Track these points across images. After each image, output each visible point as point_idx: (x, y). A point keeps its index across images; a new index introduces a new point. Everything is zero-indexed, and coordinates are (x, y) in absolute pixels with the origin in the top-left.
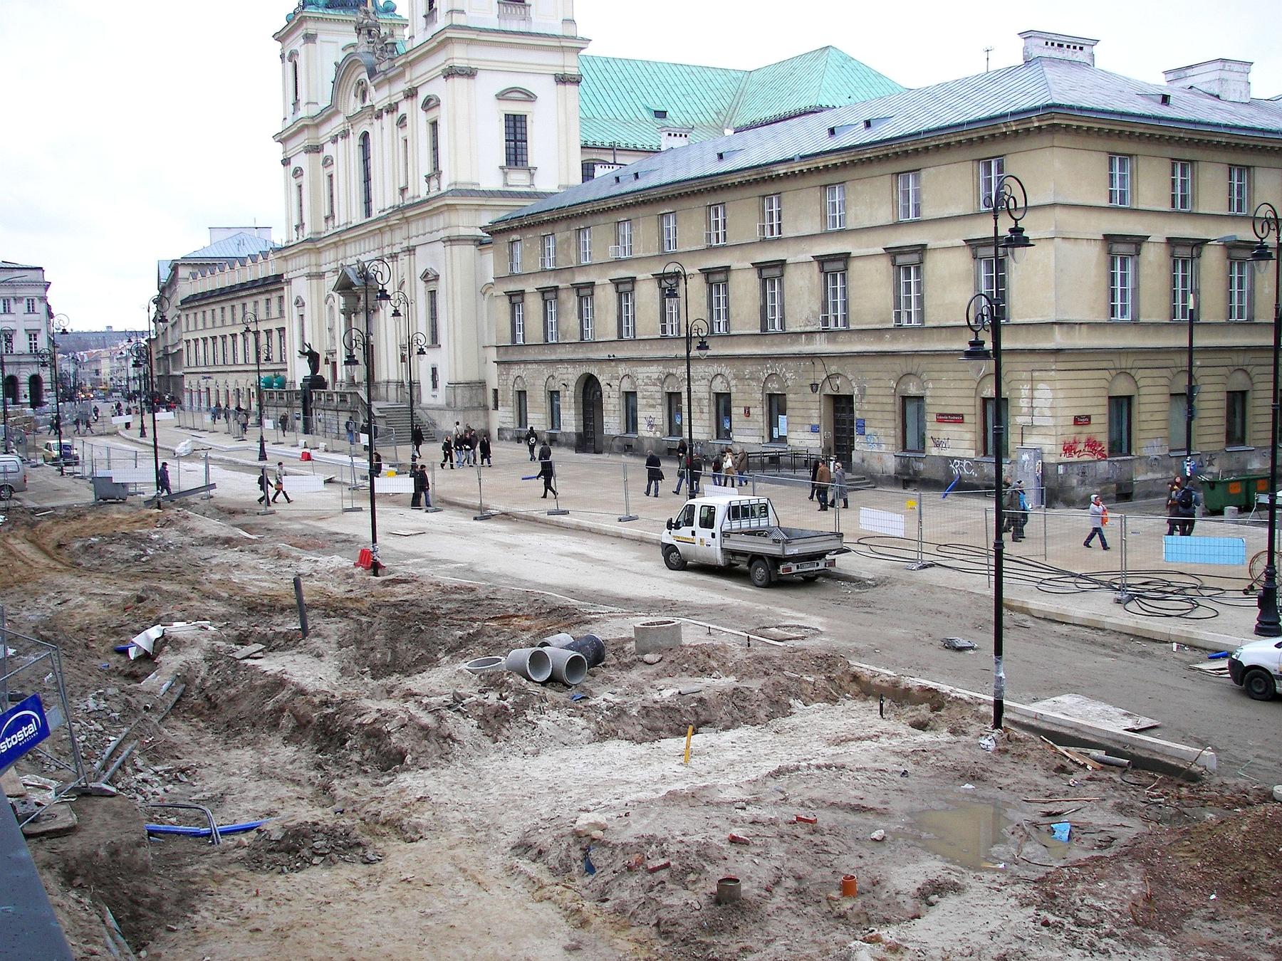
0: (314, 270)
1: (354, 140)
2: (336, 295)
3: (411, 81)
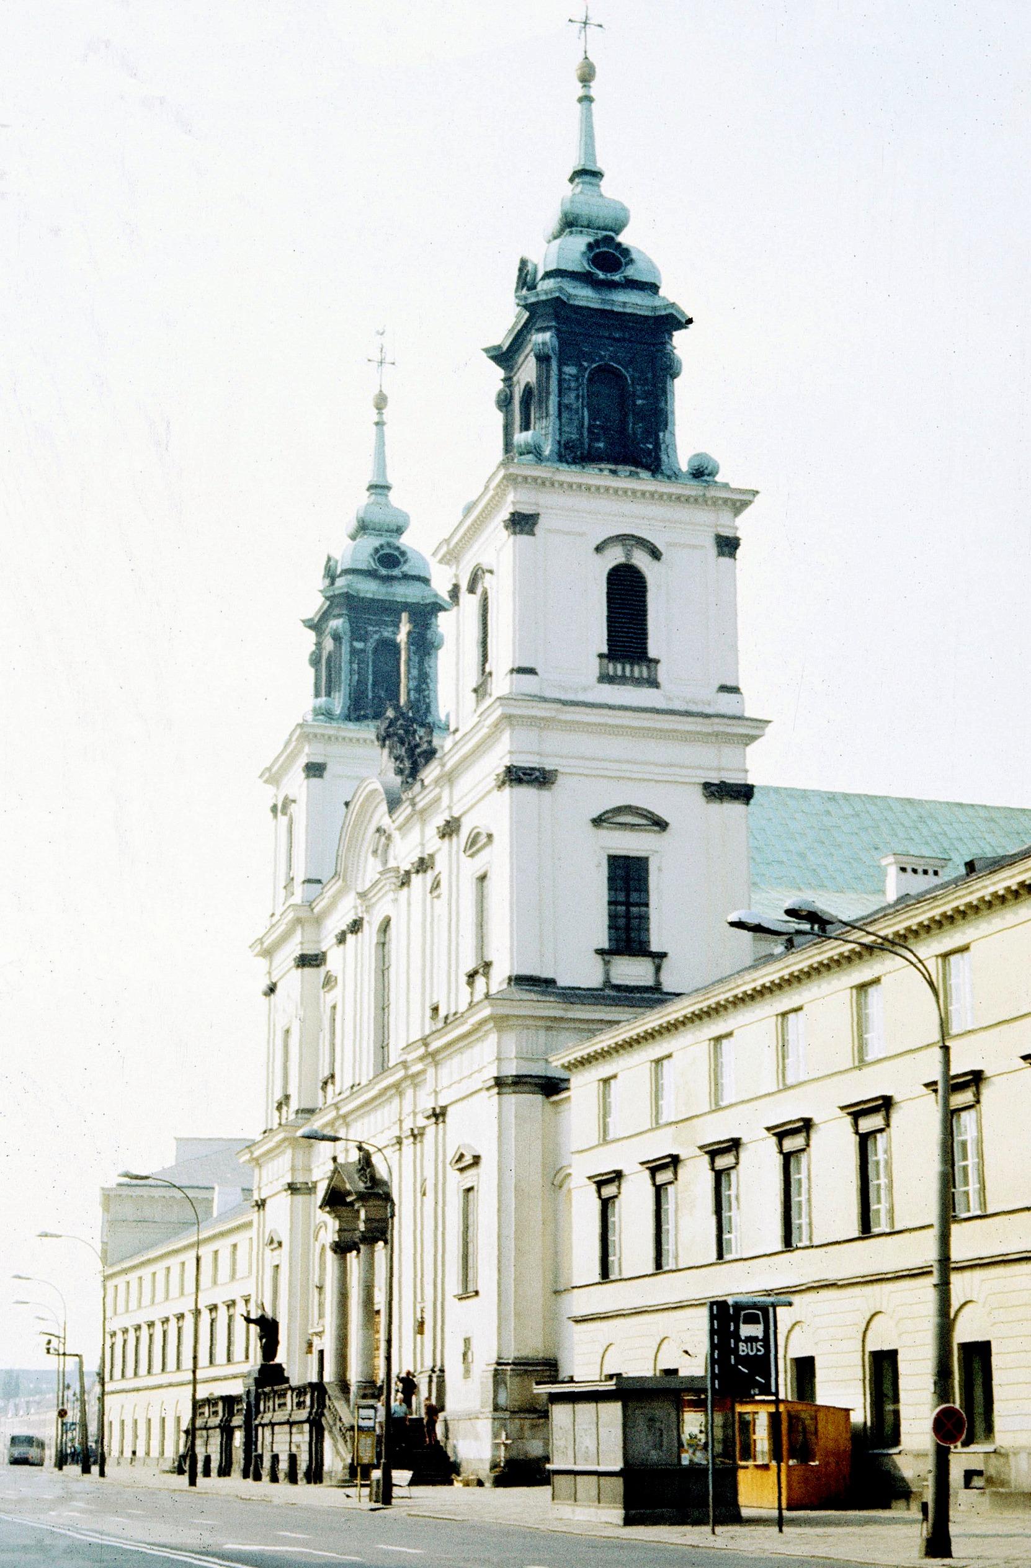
1: (370, 931)
3: (450, 808)
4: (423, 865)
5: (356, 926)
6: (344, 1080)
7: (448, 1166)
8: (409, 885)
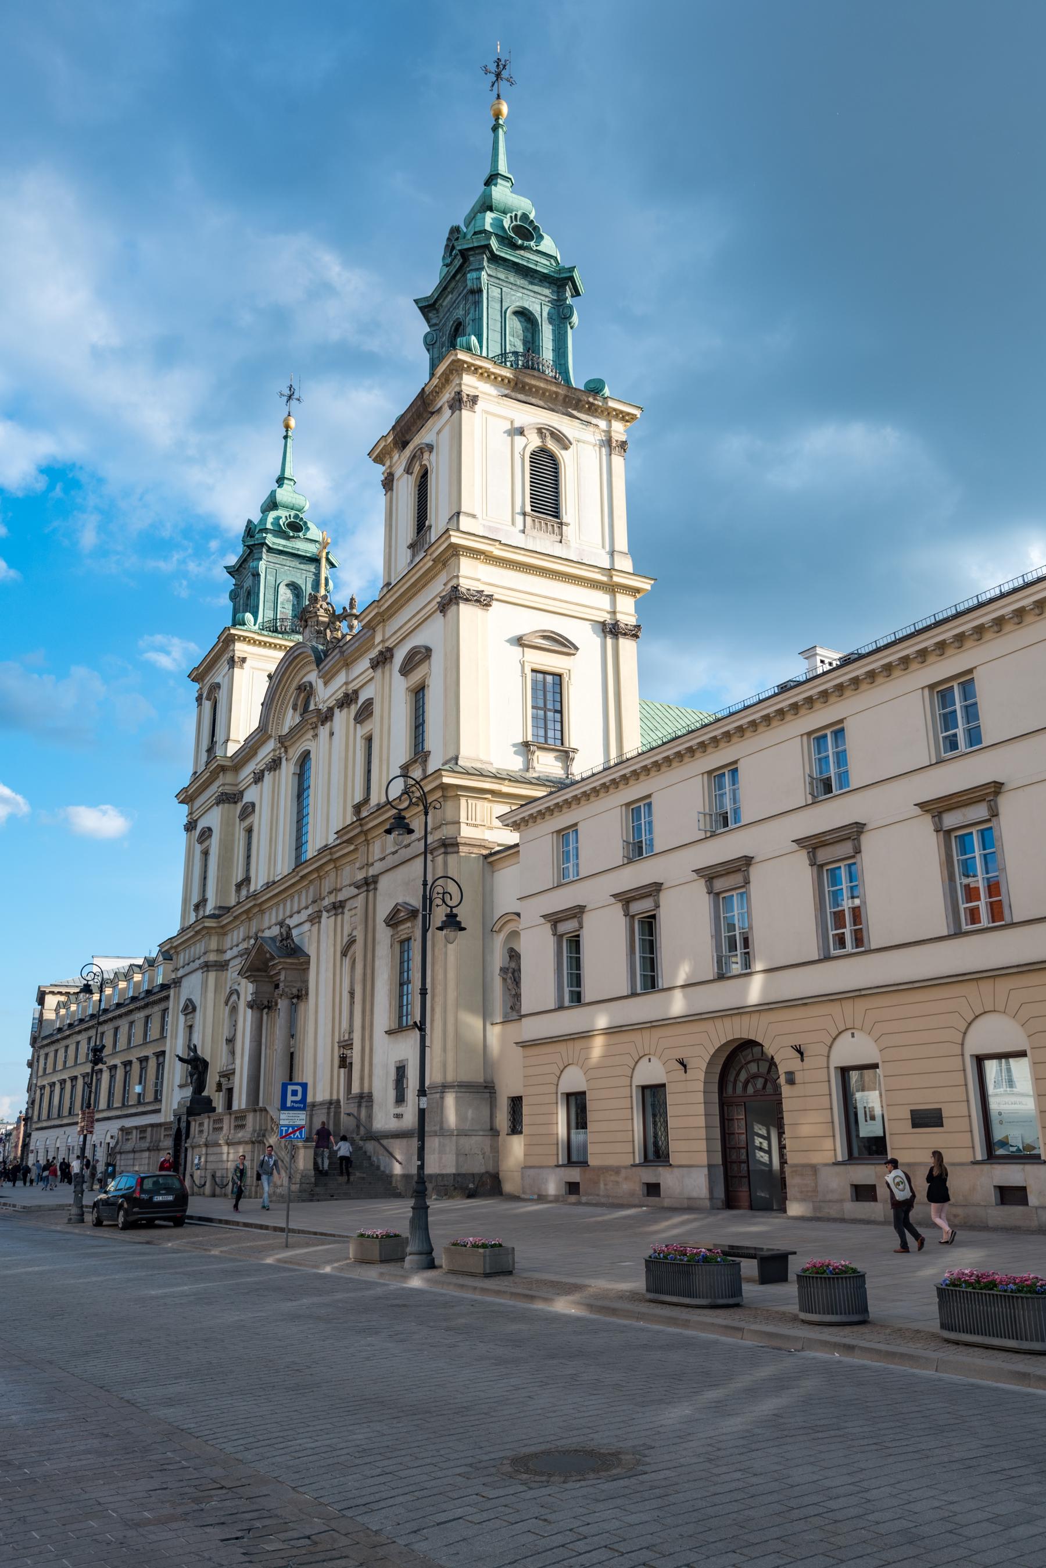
0: (212, 957)
1: (288, 769)
2: (244, 981)
3: (383, 641)
4: (347, 700)
5: (275, 765)
6: (258, 882)
7: (381, 925)
8: (332, 720)
